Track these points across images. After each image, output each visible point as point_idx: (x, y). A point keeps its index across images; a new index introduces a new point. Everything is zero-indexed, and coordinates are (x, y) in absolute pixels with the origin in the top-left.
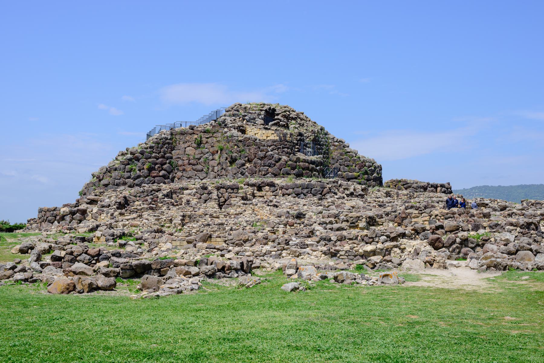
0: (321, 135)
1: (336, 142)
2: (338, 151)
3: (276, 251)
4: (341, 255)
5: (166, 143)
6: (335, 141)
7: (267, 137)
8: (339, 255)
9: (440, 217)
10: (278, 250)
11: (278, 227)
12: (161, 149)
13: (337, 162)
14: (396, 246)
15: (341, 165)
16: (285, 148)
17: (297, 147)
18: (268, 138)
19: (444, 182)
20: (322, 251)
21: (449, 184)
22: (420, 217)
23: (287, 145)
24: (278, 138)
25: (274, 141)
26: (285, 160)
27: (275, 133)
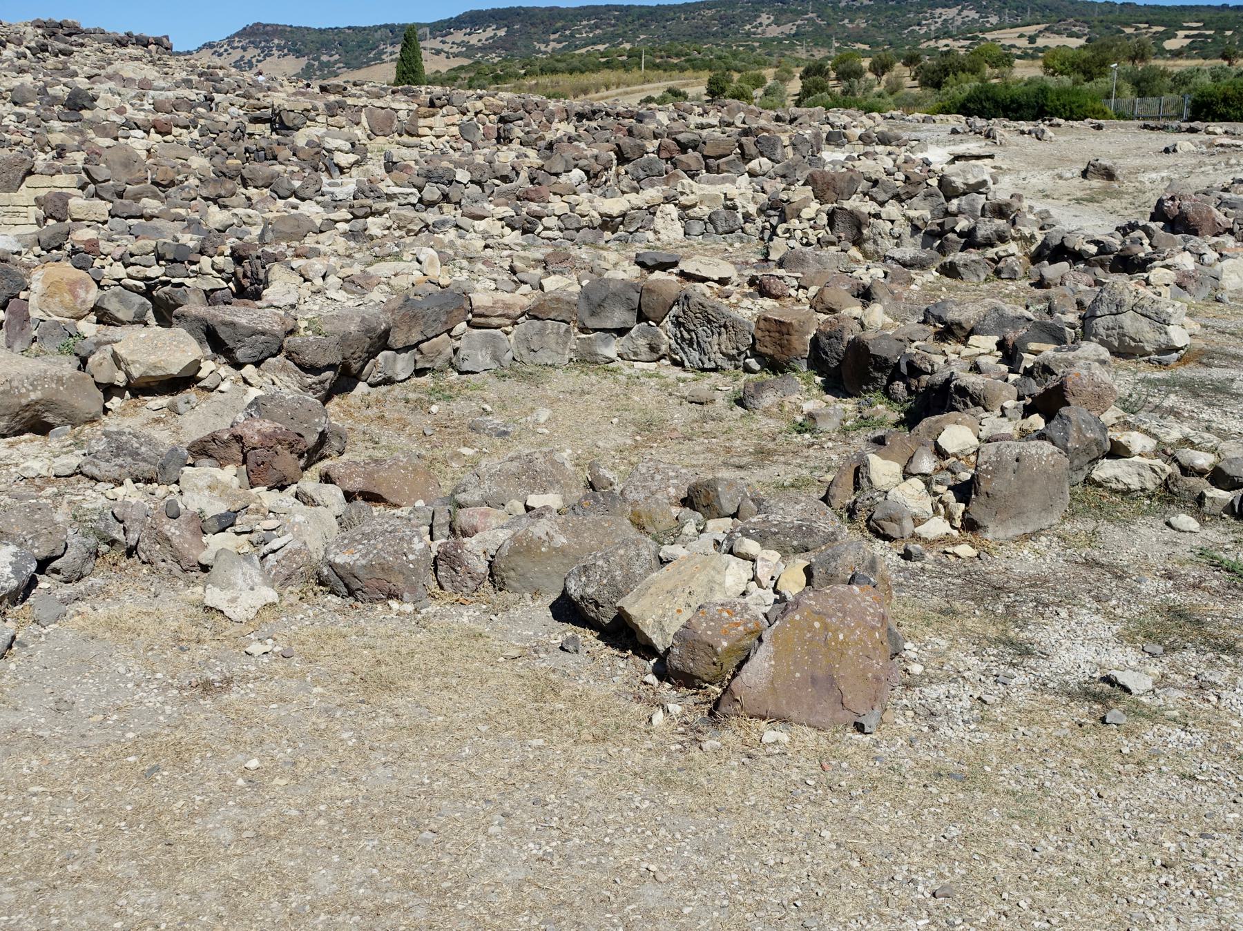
3: (347, 221)
4: (546, 229)
8: (540, 228)
9: (487, 115)
10: (356, 217)
11: (127, 138)
14: (667, 200)
19: (159, 35)
20: (501, 219)
21: (167, 37)
22: (438, 117)
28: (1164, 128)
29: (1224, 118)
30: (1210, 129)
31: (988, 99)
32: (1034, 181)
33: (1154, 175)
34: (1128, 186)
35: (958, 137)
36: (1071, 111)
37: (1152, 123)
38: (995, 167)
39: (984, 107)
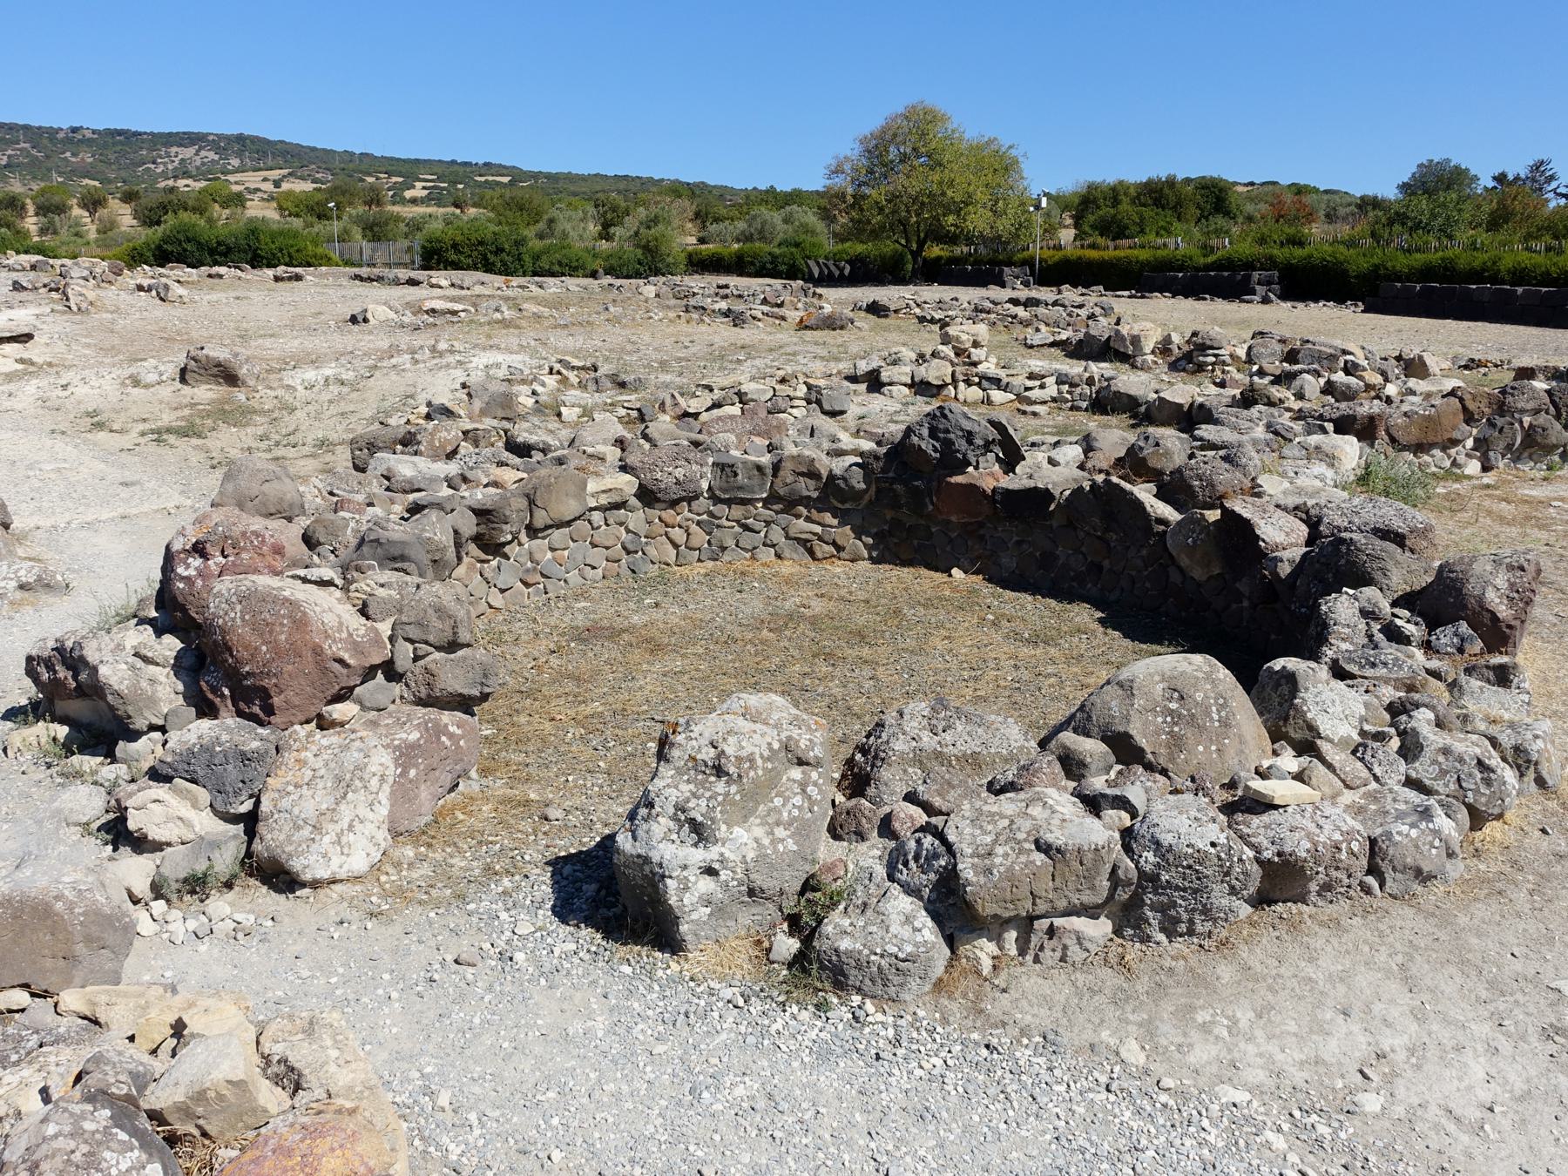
28: (379, 279)
29: (457, 266)
30: (434, 281)
31: (188, 240)
32: (81, 391)
33: (310, 374)
34: (265, 397)
35: (23, 295)
36: (290, 256)
37: (364, 271)
38: (21, 361)
39: (185, 250)
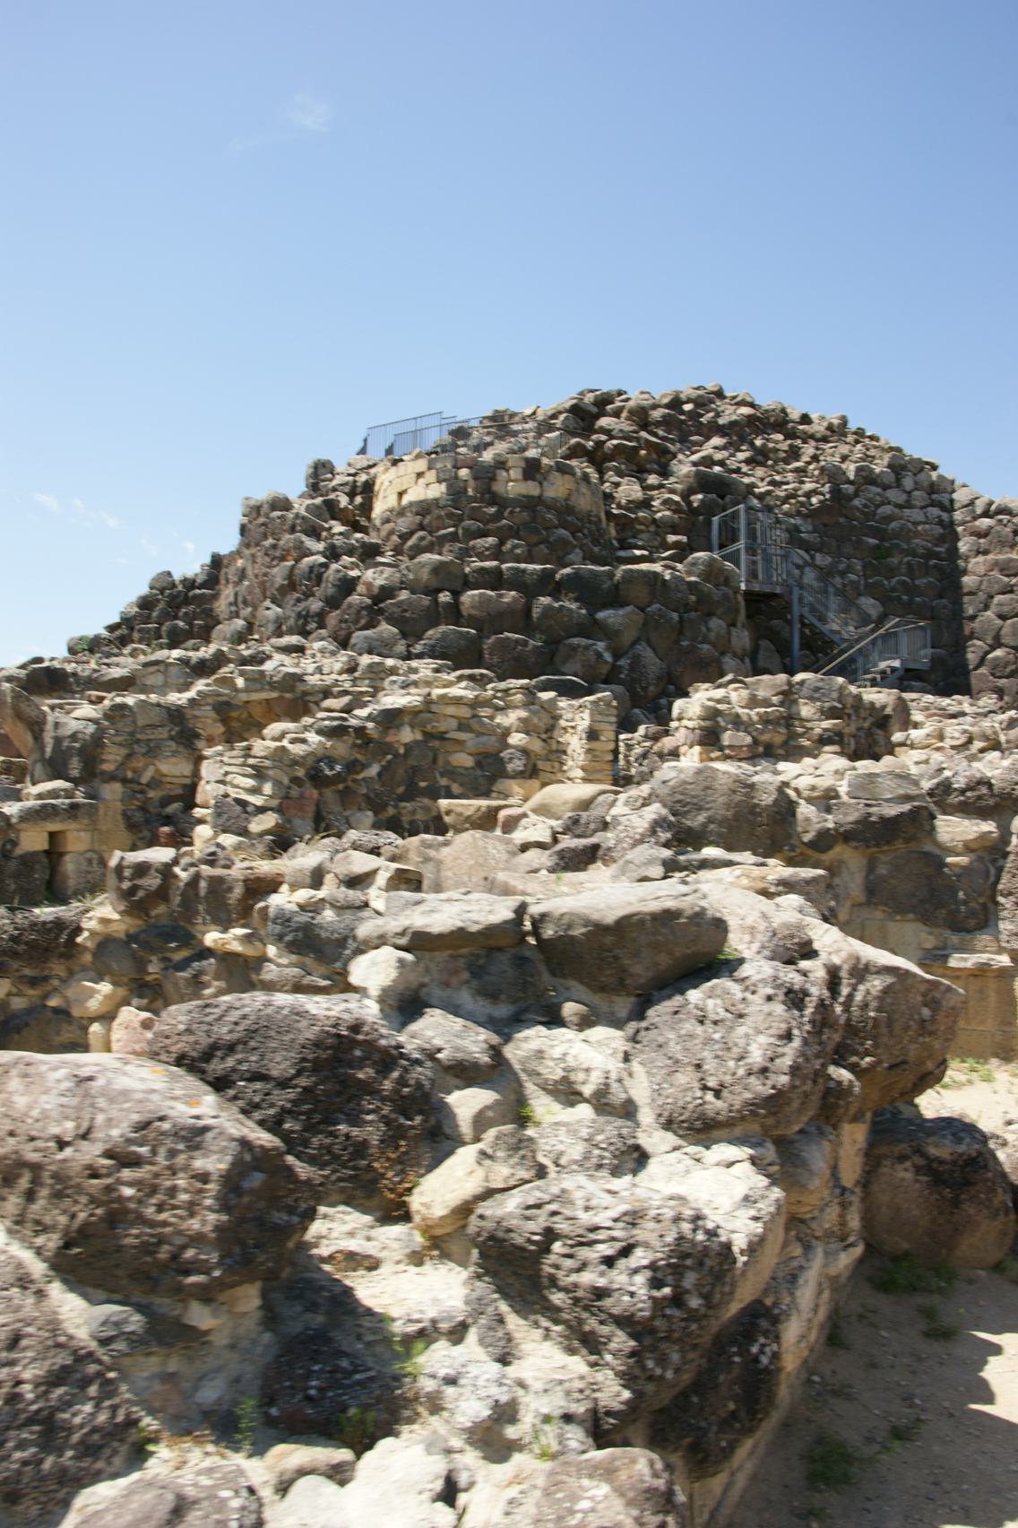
0: (894, 495)
1: (986, 514)
2: (990, 557)
5: (187, 601)
6: (979, 511)
7: (401, 495)
12: (161, 624)
13: (986, 608)
15: (1003, 617)
16: (484, 535)
17: (672, 538)
18: (406, 500)
23: (498, 516)
24: (437, 491)
25: (424, 508)
26: (369, 585)
27: (430, 469)
